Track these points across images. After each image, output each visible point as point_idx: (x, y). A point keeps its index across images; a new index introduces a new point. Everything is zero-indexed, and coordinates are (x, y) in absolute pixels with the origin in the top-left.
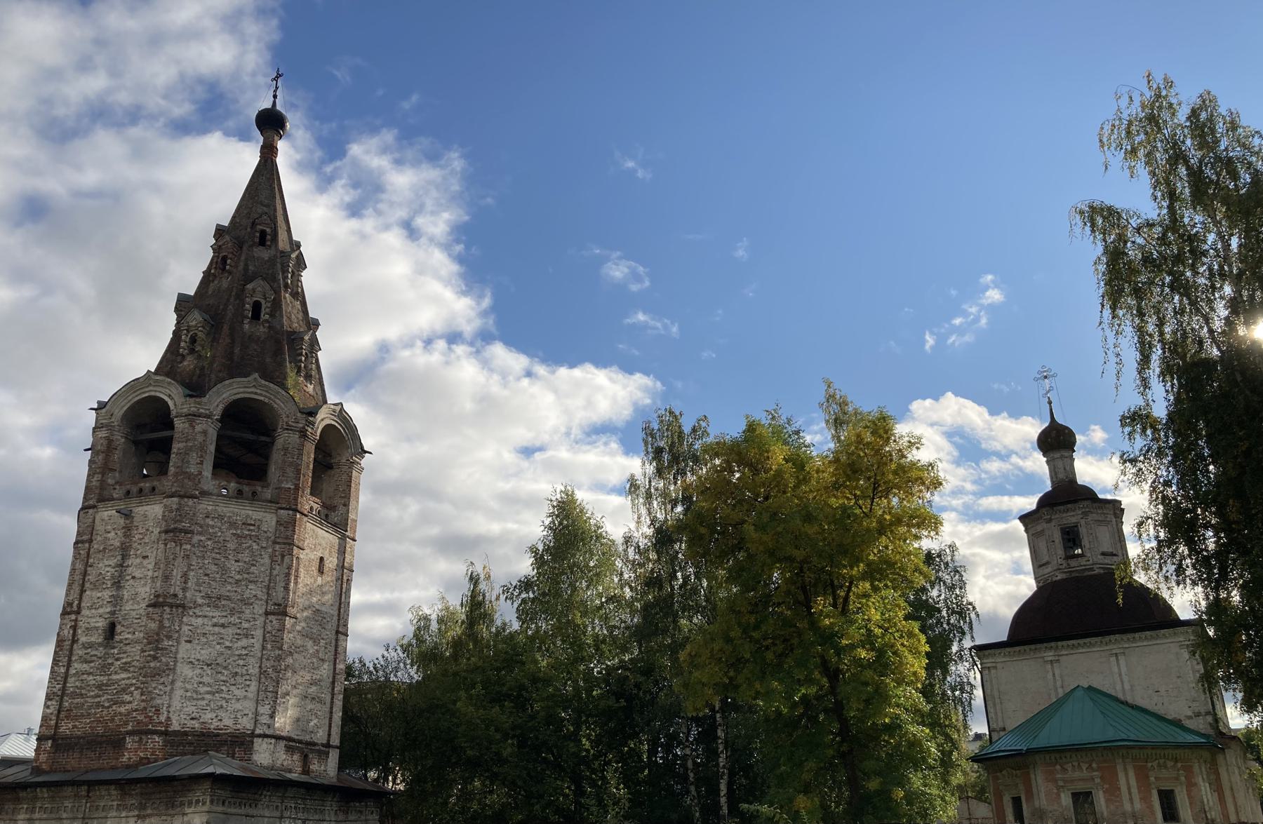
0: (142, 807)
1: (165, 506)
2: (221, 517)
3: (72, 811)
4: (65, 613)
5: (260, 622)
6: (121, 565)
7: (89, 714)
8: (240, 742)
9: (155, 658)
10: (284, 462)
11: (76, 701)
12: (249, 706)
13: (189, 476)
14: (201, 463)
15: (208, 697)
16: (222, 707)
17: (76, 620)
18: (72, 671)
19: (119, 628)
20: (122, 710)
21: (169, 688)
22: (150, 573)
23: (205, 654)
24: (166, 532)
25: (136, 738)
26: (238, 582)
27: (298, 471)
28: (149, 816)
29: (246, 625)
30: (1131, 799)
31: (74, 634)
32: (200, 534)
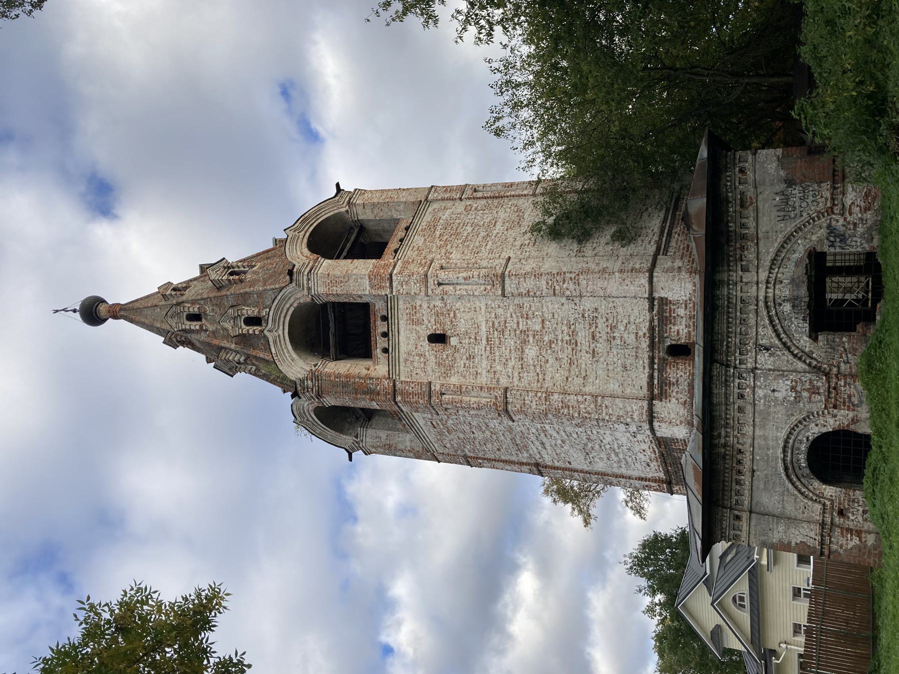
15: (621, 456)
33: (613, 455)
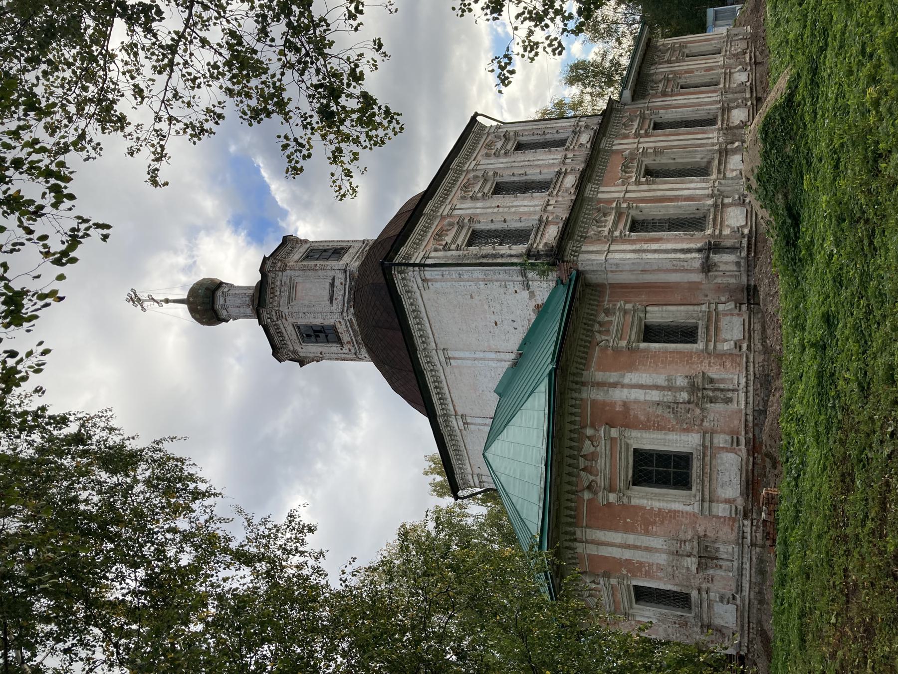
30: (647, 549)
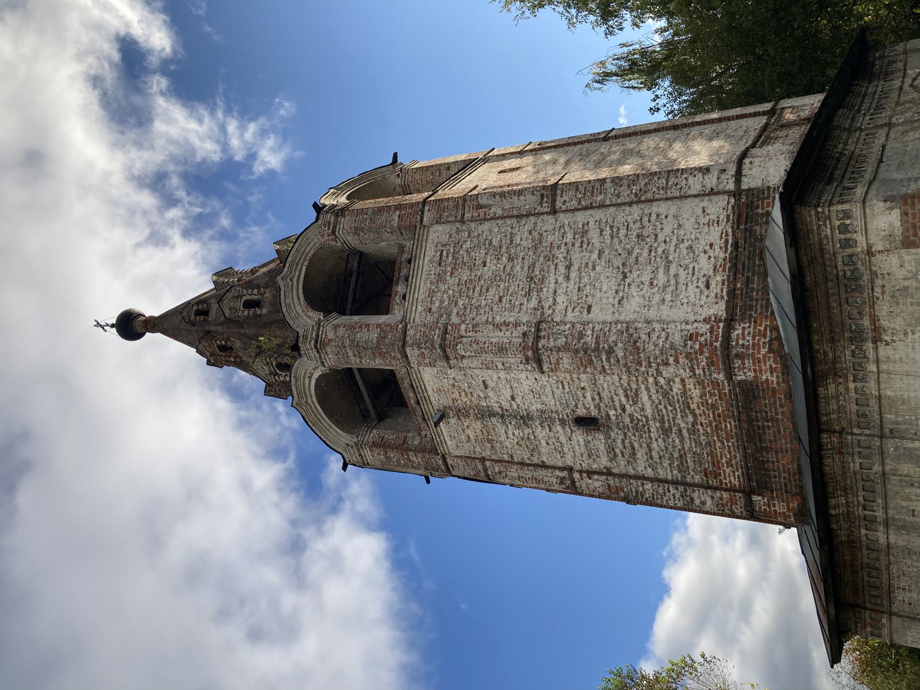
0: (858, 337)
1: (419, 364)
2: (431, 294)
3: (868, 457)
4: (573, 489)
5: (564, 218)
6: (502, 416)
7: (708, 444)
8: (746, 208)
9: (610, 351)
10: (370, 230)
11: (691, 464)
12: (689, 208)
13: (382, 338)
14: (368, 326)
15: (673, 271)
16: (690, 248)
17: (580, 472)
18: (650, 473)
19: (581, 412)
20: (696, 393)
21: (657, 326)
22: (502, 374)
23: (608, 284)
24: (447, 359)
25: (737, 363)
26: (511, 259)
27: (381, 210)
28: (874, 319)
29: (570, 236)
31: (600, 473)
32: (449, 315)
33: (661, 270)
